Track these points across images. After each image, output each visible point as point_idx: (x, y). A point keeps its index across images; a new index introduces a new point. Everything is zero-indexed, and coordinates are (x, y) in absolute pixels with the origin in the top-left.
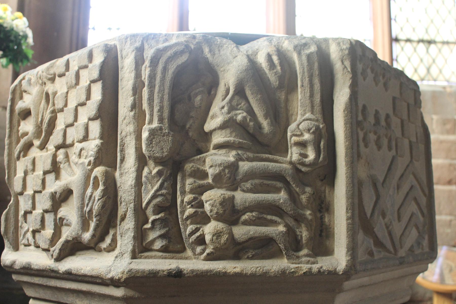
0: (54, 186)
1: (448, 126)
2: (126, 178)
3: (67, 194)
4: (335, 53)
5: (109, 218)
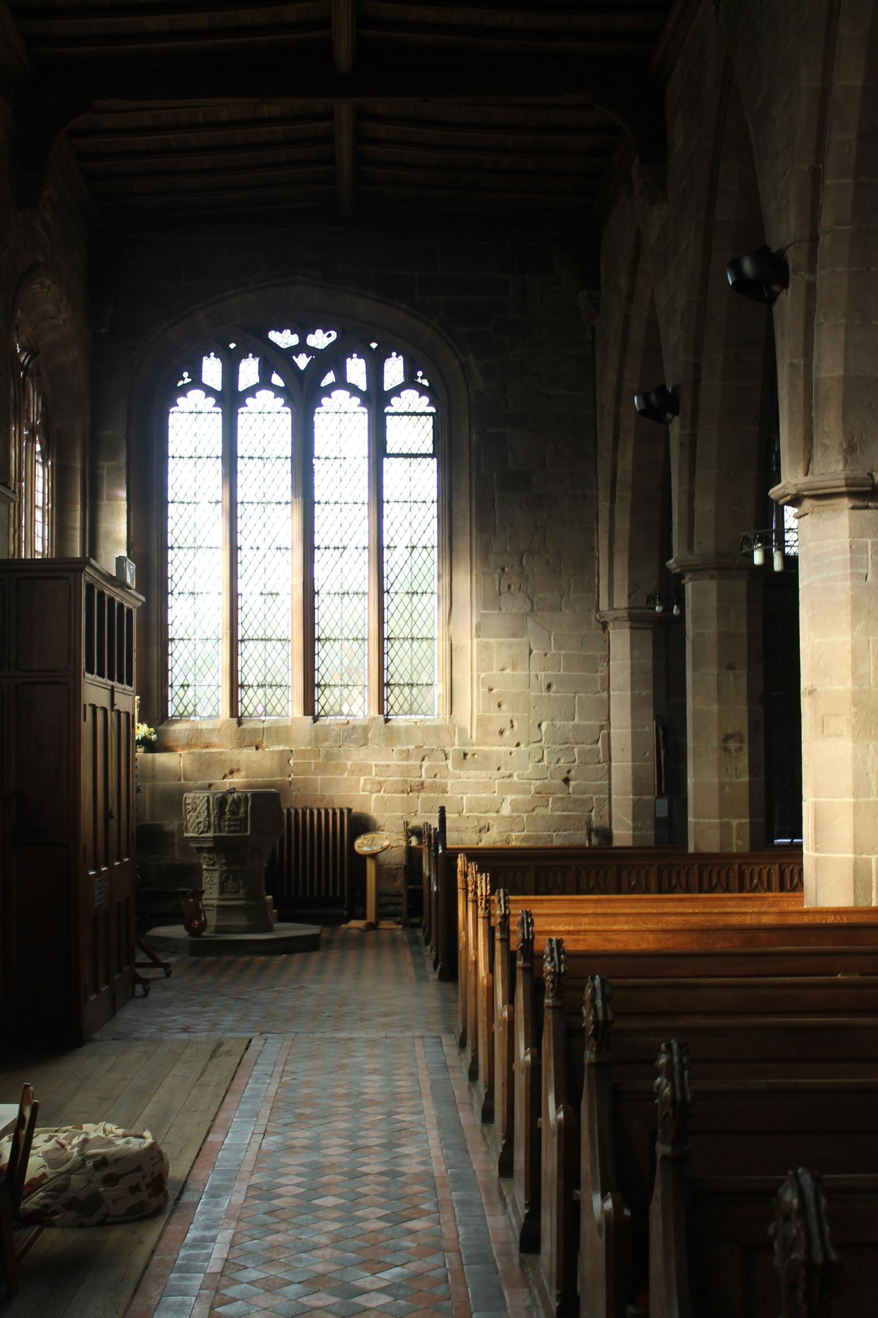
0: (197, 821)
1: (403, 756)
2: (212, 819)
3: (200, 822)
4: (249, 795)
5: (209, 827)
